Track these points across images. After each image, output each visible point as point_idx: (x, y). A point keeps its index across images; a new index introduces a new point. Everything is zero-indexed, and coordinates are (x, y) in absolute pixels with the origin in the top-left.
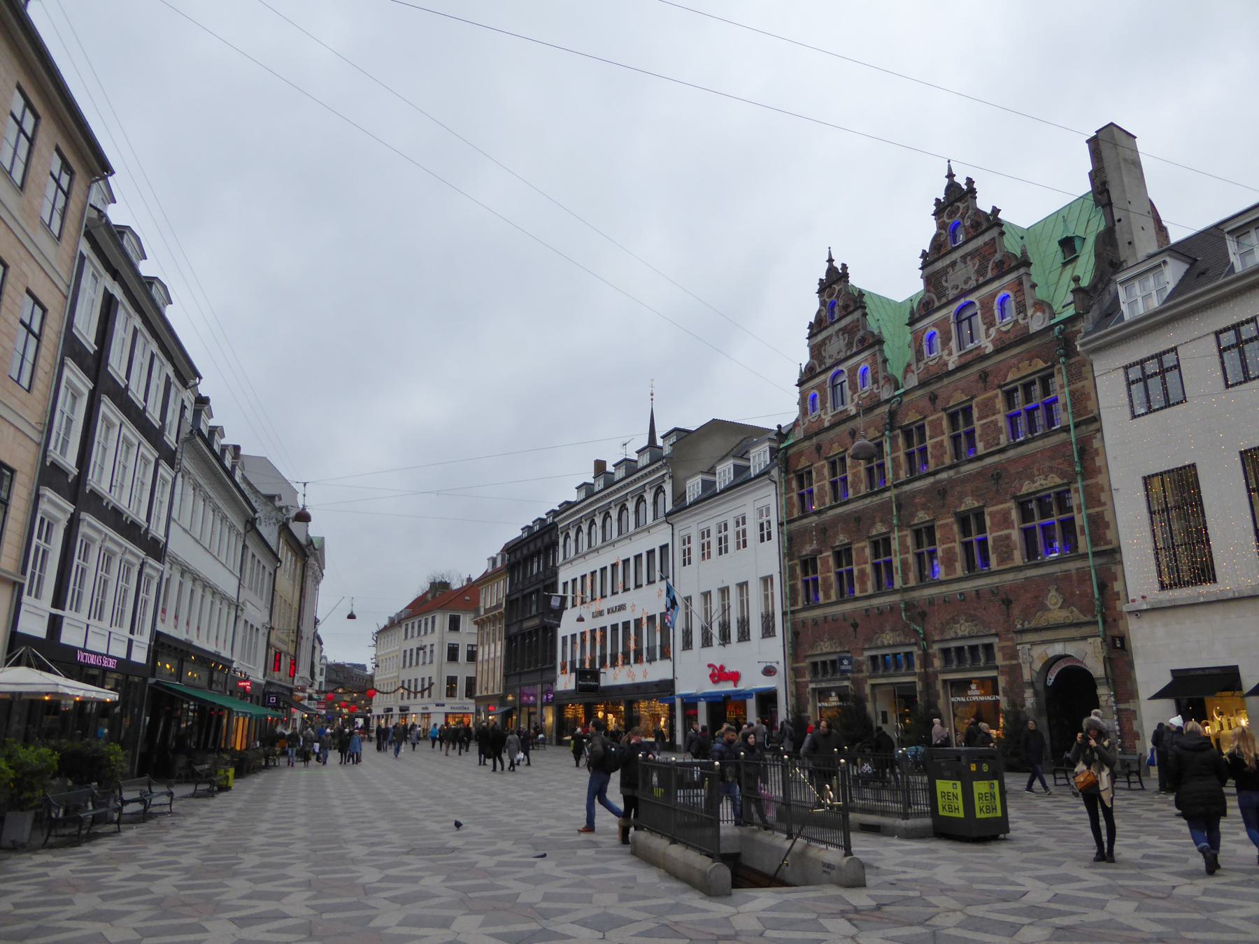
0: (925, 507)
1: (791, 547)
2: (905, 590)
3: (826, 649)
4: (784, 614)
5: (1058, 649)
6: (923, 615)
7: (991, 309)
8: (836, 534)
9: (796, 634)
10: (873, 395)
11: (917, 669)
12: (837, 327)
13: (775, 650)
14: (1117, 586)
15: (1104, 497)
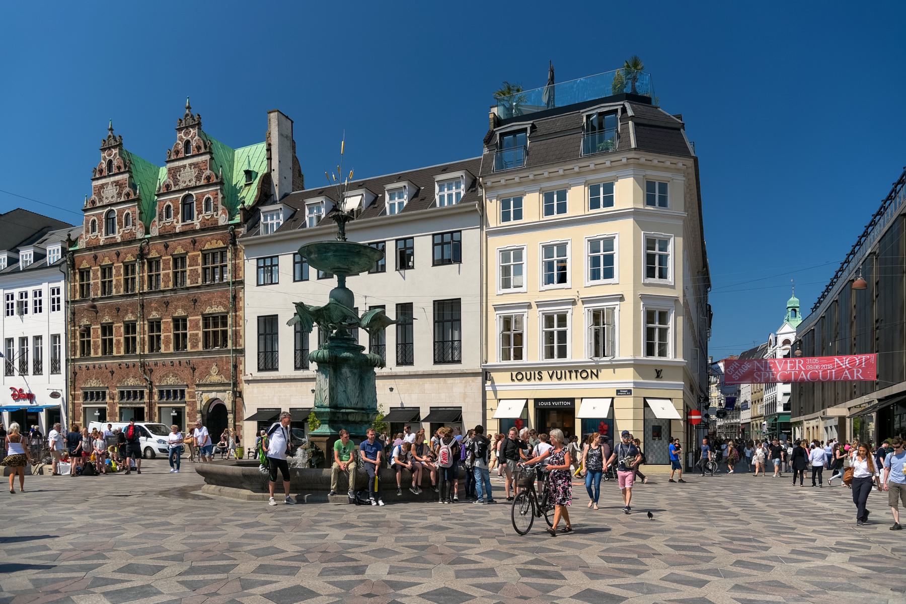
0: (156, 309)
1: (72, 319)
2: (141, 356)
3: (93, 384)
4: (67, 360)
5: (213, 395)
6: (151, 371)
7: (201, 203)
8: (104, 316)
9: (75, 373)
10: (132, 234)
11: (146, 400)
12: (112, 179)
13: (59, 382)
14: (241, 367)
15: (241, 322)
